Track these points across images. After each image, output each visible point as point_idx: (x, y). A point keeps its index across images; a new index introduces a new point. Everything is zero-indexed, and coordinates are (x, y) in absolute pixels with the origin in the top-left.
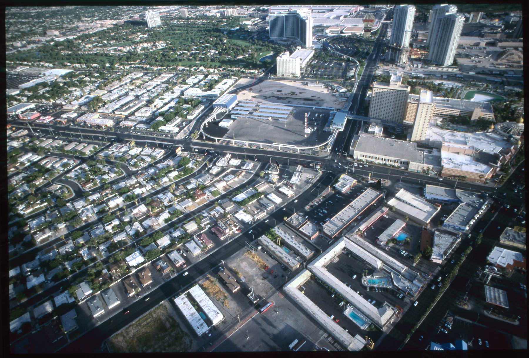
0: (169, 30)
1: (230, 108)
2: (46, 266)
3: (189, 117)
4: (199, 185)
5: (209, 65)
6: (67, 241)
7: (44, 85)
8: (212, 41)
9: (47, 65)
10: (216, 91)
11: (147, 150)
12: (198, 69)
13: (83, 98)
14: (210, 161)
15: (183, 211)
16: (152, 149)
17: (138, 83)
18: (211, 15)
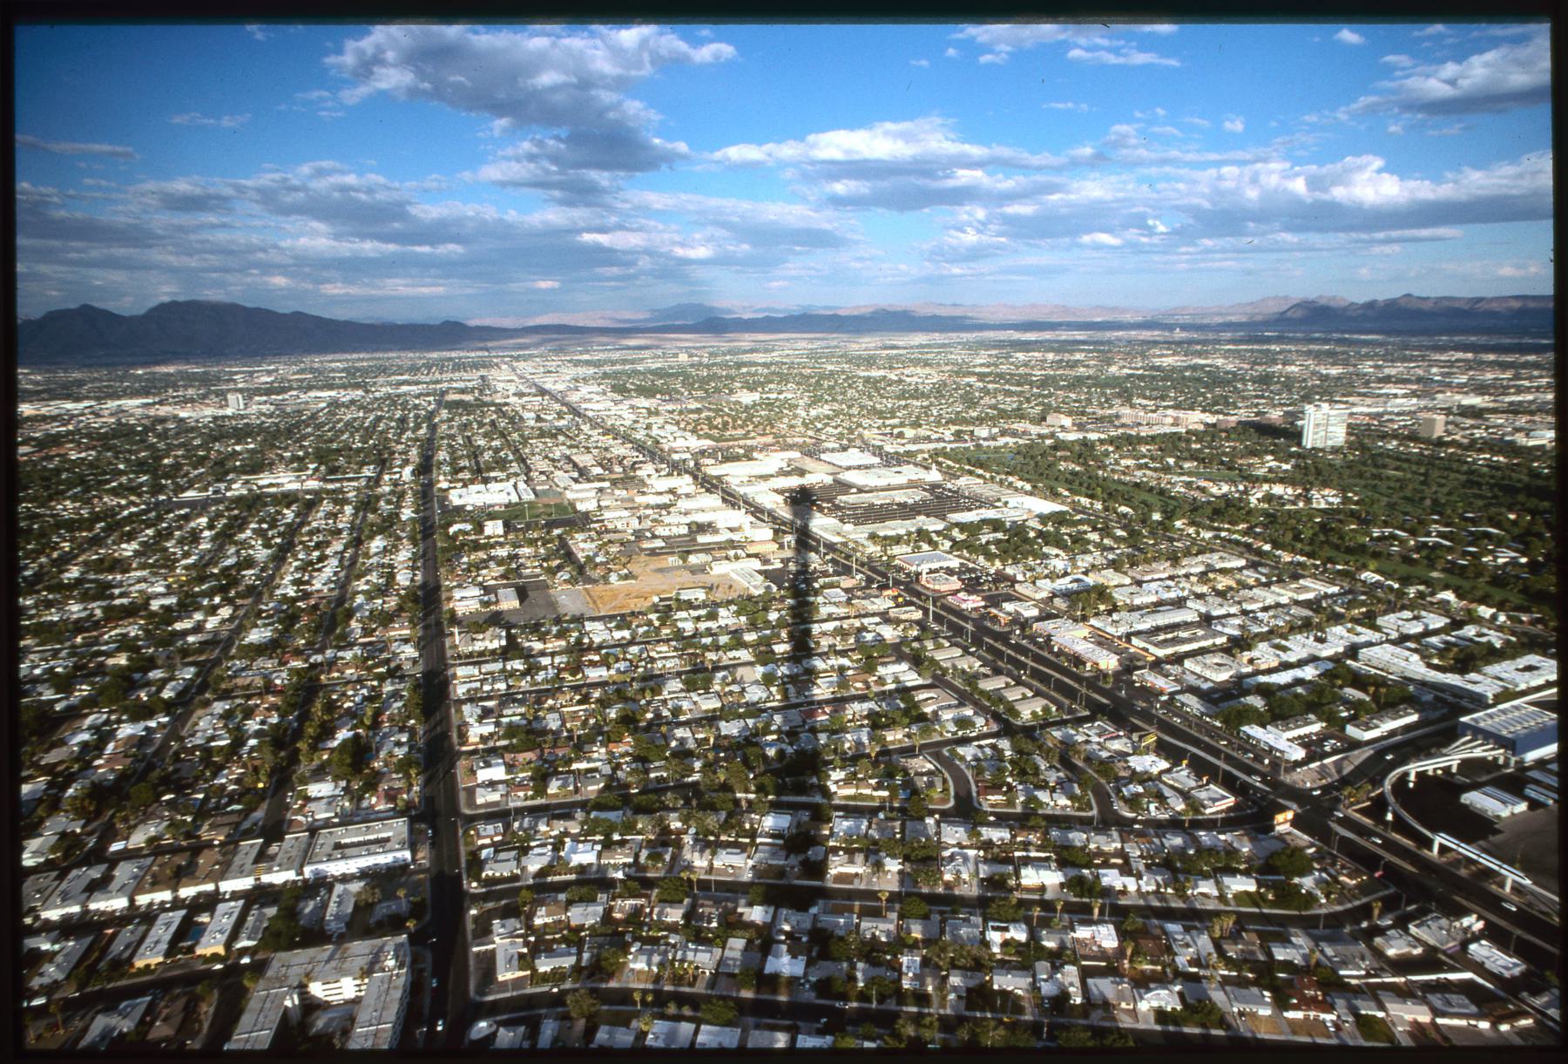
0: (1364, 464)
1: (1531, 756)
2: (819, 944)
3: (1351, 730)
4: (1318, 964)
5: (1479, 594)
6: (888, 909)
7: (996, 525)
8: (1514, 523)
9: (1020, 484)
10: (1483, 682)
11: (1183, 776)
12: (1433, 594)
13: (1068, 579)
14: (1389, 905)
15: (1229, 1018)
16: (1199, 777)
17: (1223, 582)
18: (1531, 443)
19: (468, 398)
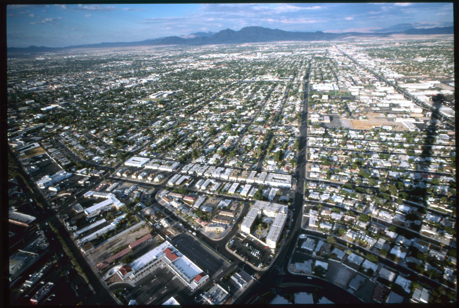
2: (412, 251)
6: (443, 250)
19: (321, 56)
